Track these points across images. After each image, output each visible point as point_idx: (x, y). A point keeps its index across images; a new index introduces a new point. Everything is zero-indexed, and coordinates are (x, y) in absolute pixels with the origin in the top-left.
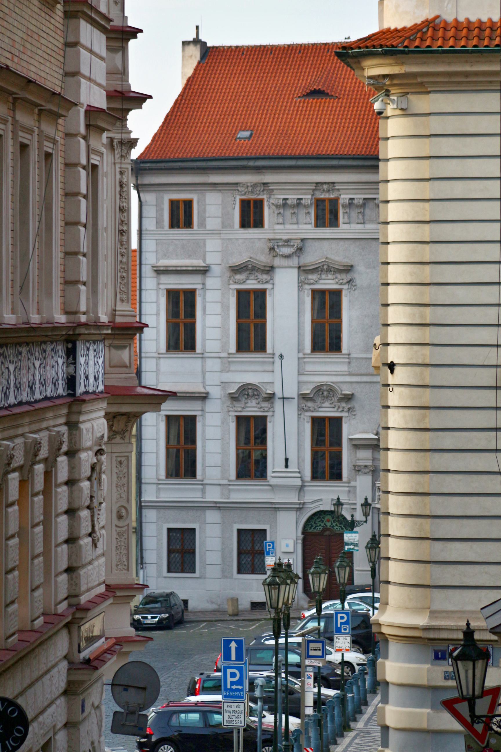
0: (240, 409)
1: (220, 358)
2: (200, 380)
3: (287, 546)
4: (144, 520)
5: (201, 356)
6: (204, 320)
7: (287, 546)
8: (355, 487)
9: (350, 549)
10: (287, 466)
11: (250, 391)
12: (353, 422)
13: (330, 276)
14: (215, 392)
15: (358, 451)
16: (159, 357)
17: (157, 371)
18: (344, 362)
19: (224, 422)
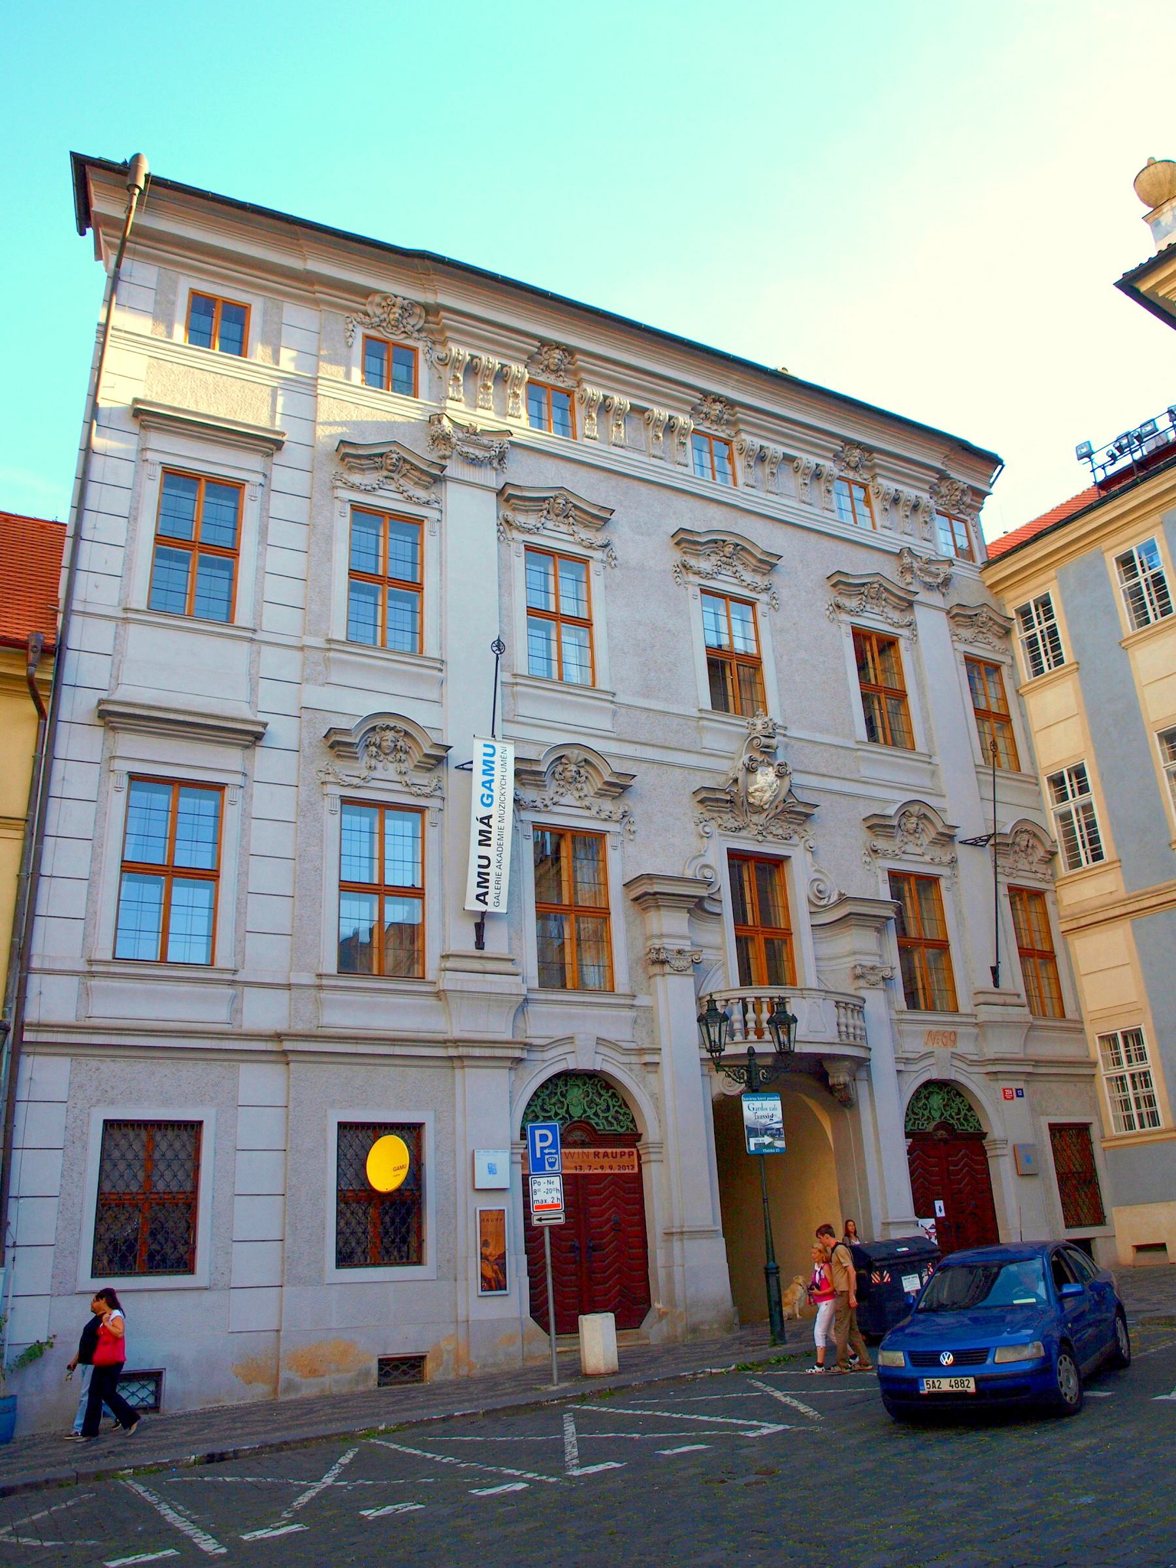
0: (356, 781)
1: (302, 648)
2: (244, 695)
3: (492, 1170)
4: (22, 1093)
5: (250, 635)
6: (261, 556)
7: (492, 1170)
8: (649, 1009)
9: (763, 1145)
10: (480, 944)
11: (390, 735)
12: (630, 849)
13: (563, 528)
14: (281, 731)
15: (652, 915)
16: (126, 617)
17: (116, 656)
18: (602, 708)
19: (305, 810)
